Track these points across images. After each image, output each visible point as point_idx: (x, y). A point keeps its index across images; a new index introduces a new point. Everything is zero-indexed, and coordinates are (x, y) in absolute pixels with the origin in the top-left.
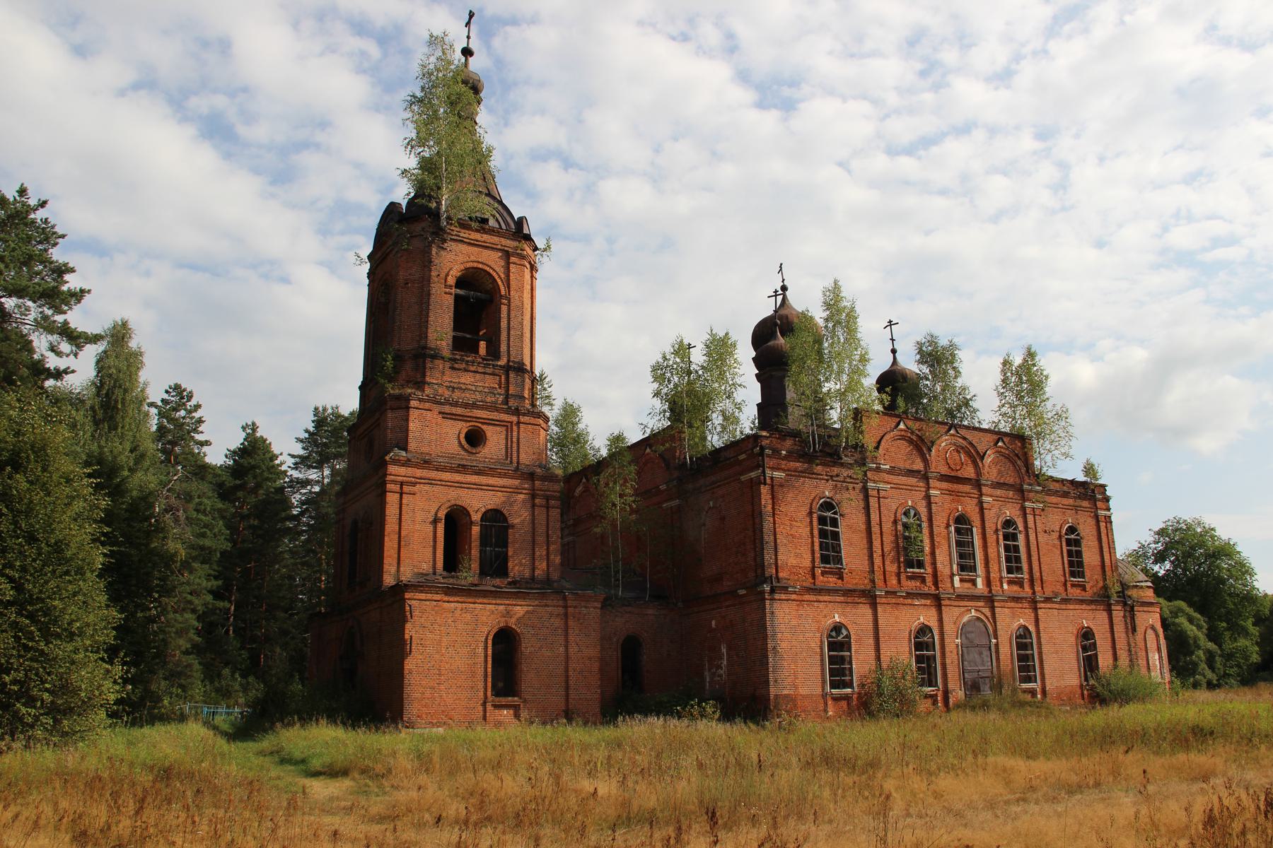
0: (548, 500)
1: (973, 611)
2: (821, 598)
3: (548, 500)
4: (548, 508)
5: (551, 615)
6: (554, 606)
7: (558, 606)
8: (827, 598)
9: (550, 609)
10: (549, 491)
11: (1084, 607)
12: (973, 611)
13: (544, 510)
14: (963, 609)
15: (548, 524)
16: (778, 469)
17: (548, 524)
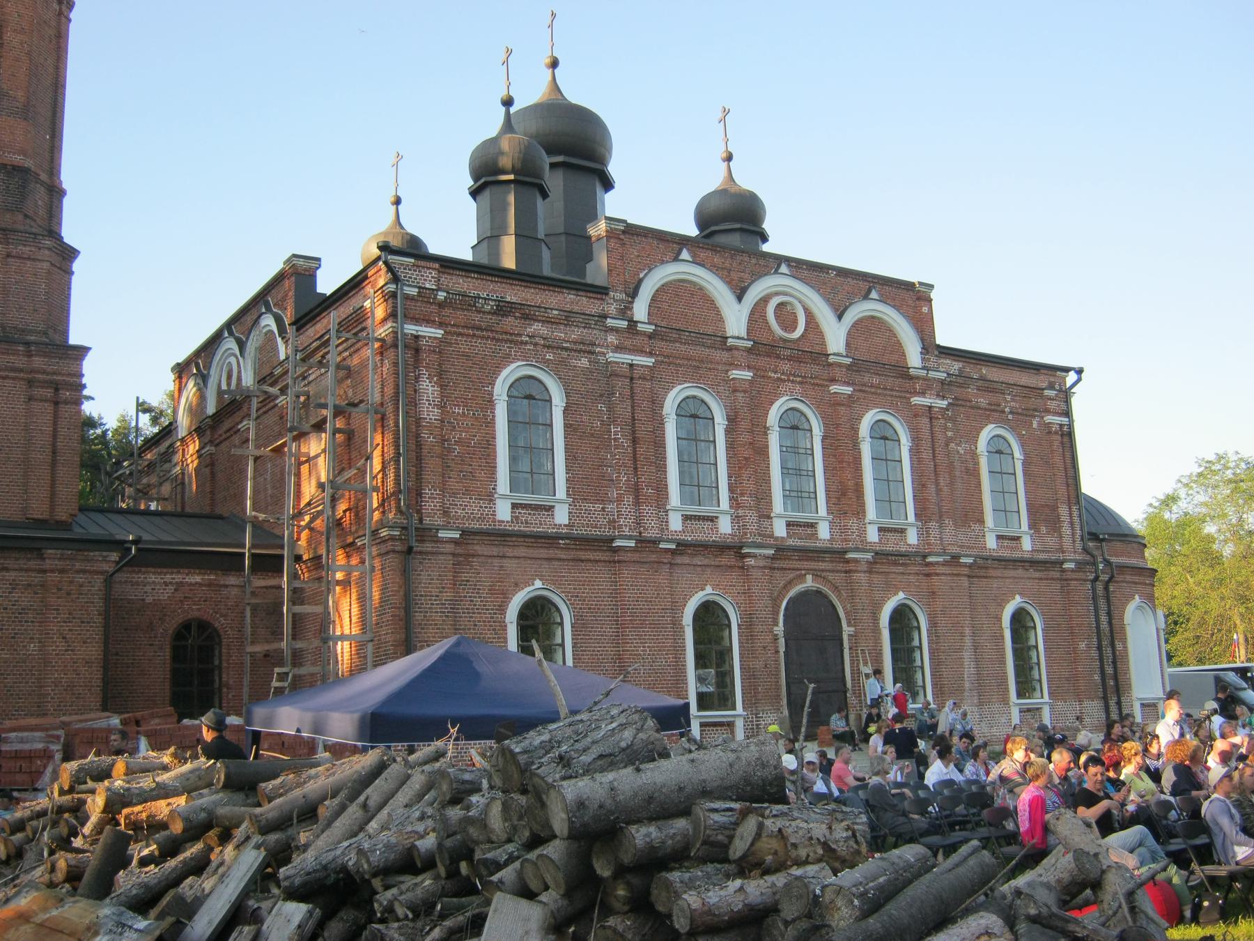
0: (57, 390)
1: (809, 577)
2: (509, 552)
3: (57, 390)
4: (56, 403)
5: (14, 586)
6: (21, 570)
7: (27, 570)
8: (521, 552)
9: (11, 575)
10: (60, 374)
11: (1020, 572)
12: (809, 577)
13: (49, 407)
14: (791, 575)
15: (55, 430)
16: (428, 321)
17: (55, 430)
